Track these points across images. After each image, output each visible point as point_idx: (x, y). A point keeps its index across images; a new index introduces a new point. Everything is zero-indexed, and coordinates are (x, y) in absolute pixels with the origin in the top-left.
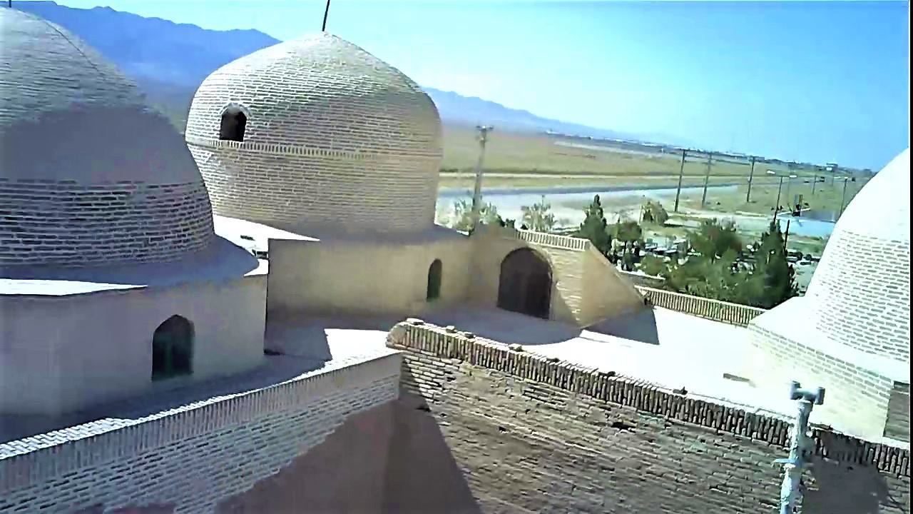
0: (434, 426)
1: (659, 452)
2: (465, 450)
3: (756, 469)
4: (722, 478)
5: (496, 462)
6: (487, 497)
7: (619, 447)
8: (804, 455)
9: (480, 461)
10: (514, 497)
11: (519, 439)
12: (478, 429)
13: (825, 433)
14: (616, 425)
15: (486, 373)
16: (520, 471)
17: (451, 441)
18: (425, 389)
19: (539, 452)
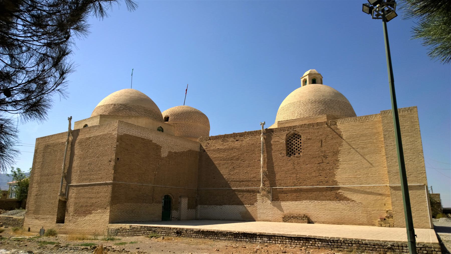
0: (207, 153)
1: (244, 142)
2: (212, 155)
3: (258, 139)
4: (253, 142)
5: (218, 155)
6: (216, 162)
7: (237, 144)
8: (264, 133)
9: (215, 156)
10: (221, 160)
11: (221, 149)
12: (214, 150)
13: (266, 129)
14: (237, 140)
15: (215, 141)
16: (222, 155)
17: (209, 155)
18: (204, 148)
19: (225, 150)
